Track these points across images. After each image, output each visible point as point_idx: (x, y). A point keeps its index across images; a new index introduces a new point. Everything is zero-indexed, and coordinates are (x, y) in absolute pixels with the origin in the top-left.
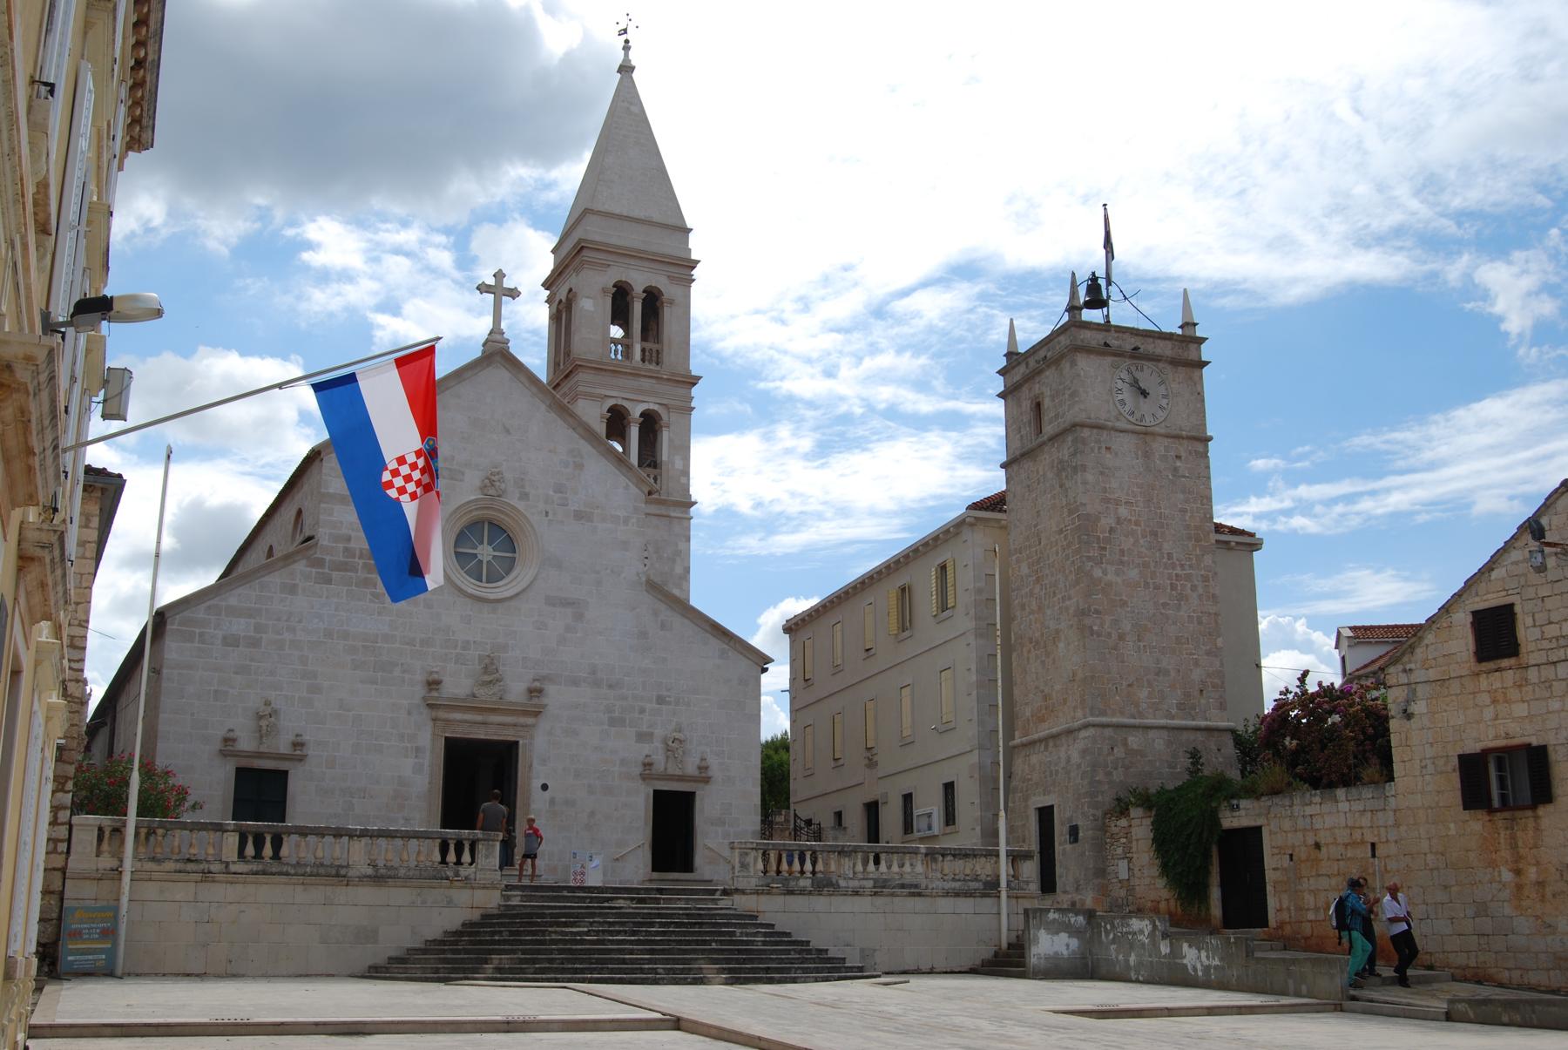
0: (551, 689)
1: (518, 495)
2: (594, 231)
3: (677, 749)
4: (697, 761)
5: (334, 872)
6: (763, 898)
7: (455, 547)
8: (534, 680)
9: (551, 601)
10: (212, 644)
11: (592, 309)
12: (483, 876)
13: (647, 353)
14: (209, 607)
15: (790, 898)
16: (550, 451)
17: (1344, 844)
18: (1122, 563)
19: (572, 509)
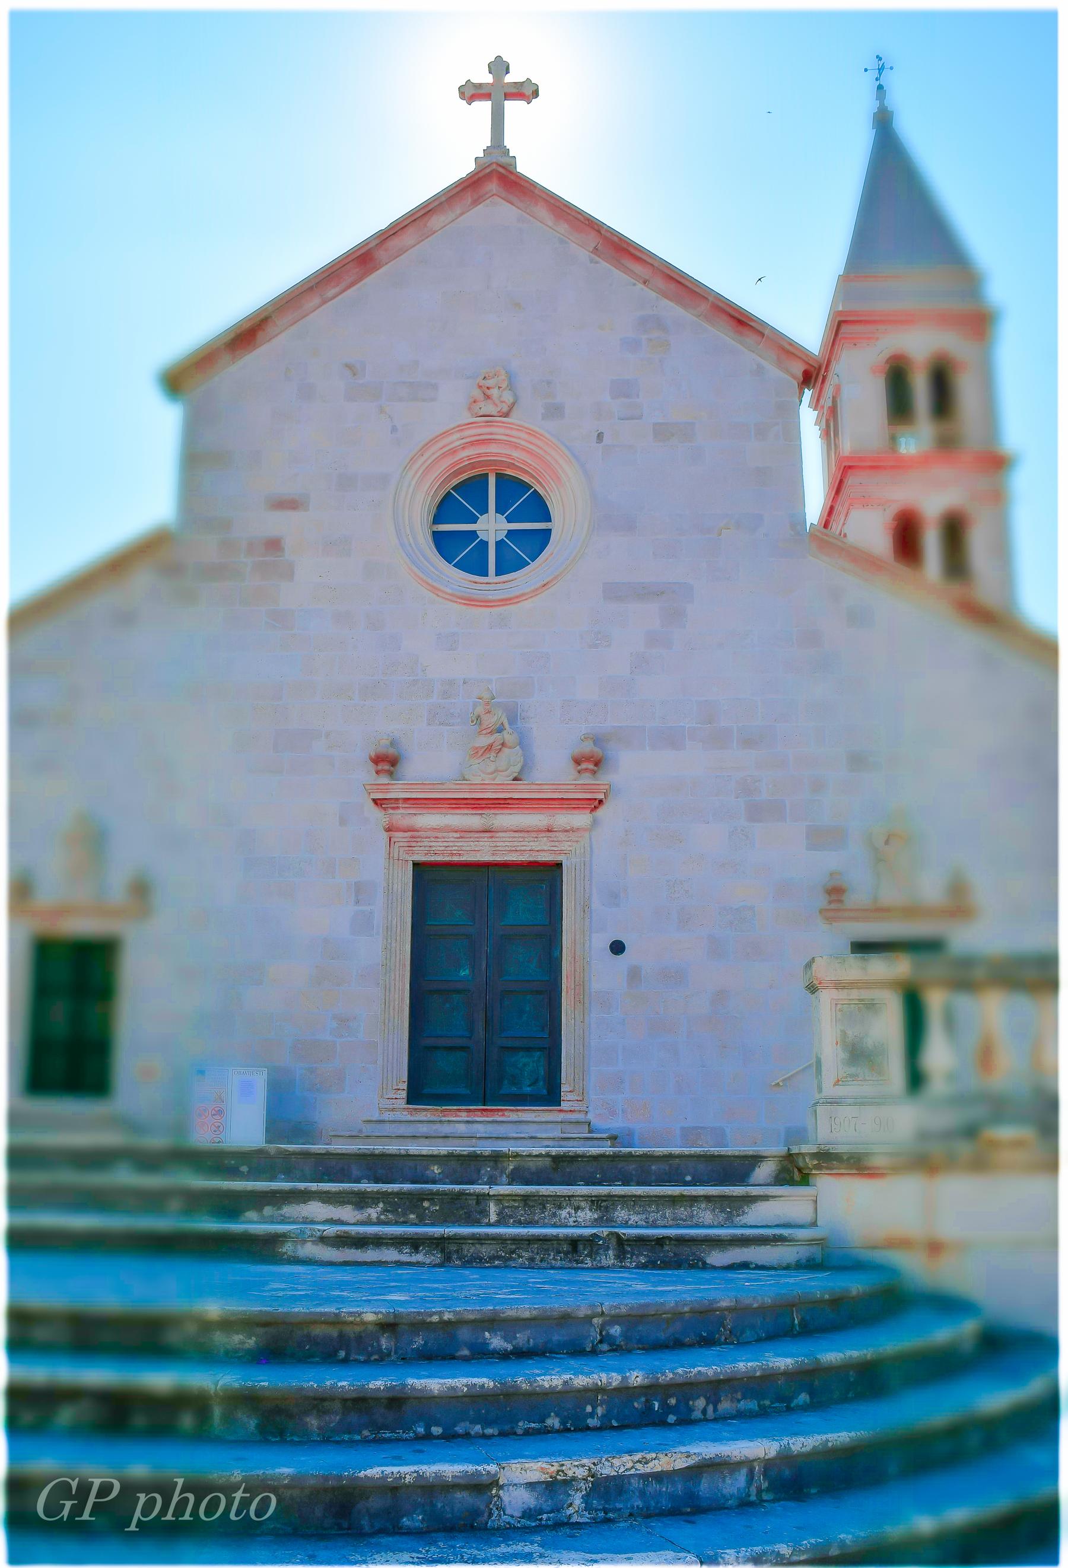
7: (437, 519)
9: (614, 592)
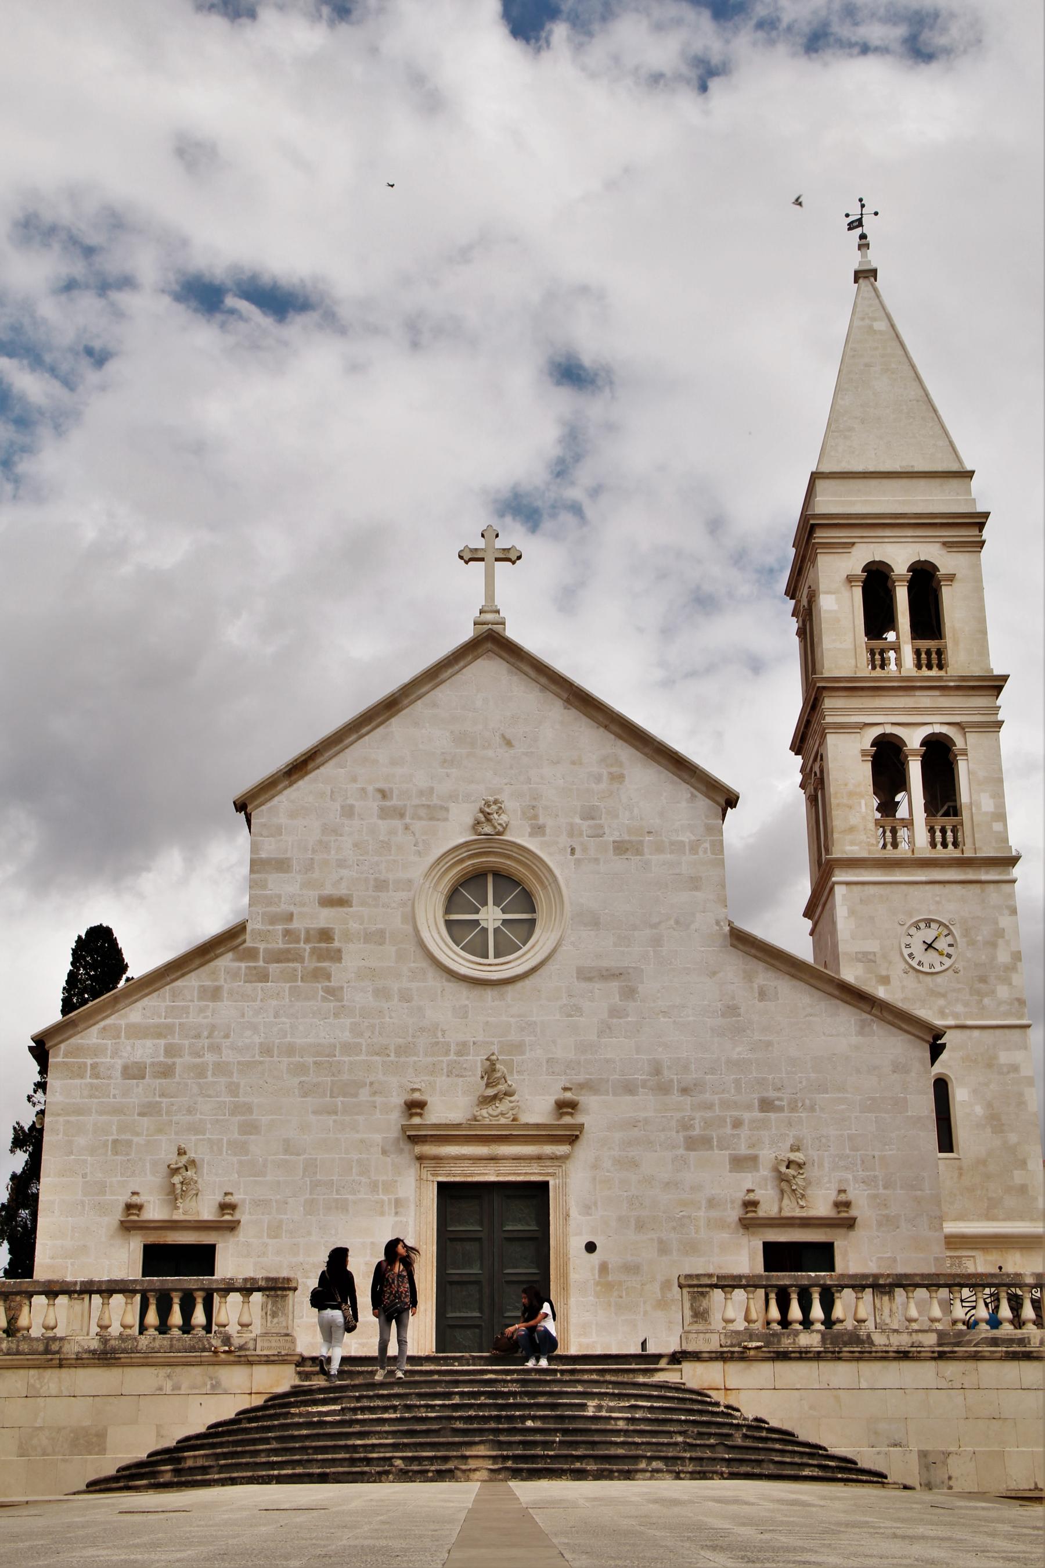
0: (588, 1100)
1: (529, 830)
2: (829, 502)
3: (794, 1177)
4: (833, 1196)
5: (41, 1348)
6: (733, 1368)
7: (448, 910)
8: (565, 1089)
9: (585, 975)
10: (110, 1077)
11: (835, 607)
12: (266, 1345)
13: (923, 656)
14: (104, 1028)
15: (782, 1367)
16: (573, 763)
19: (611, 839)
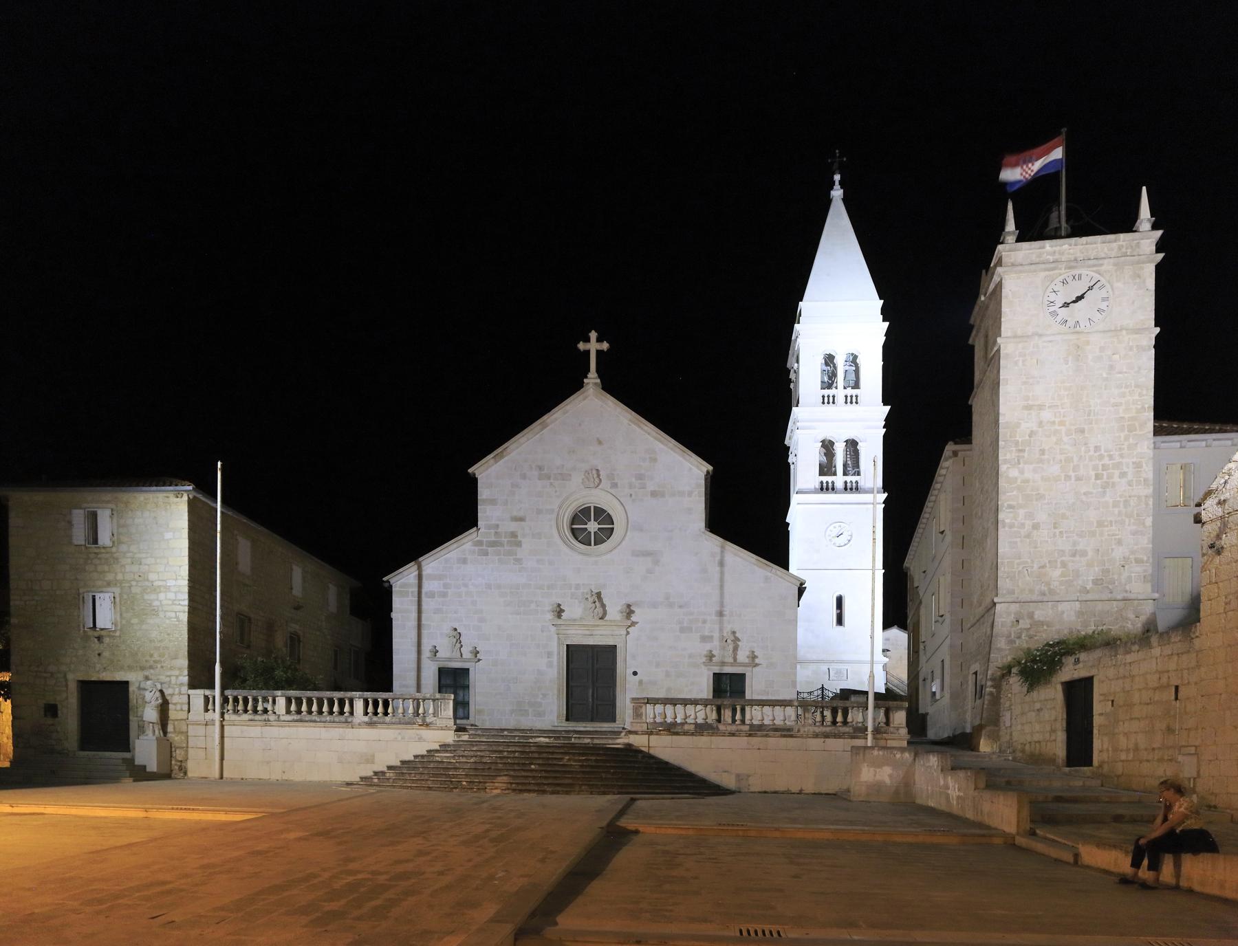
17: (1153, 689)
18: (1041, 461)
